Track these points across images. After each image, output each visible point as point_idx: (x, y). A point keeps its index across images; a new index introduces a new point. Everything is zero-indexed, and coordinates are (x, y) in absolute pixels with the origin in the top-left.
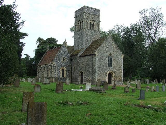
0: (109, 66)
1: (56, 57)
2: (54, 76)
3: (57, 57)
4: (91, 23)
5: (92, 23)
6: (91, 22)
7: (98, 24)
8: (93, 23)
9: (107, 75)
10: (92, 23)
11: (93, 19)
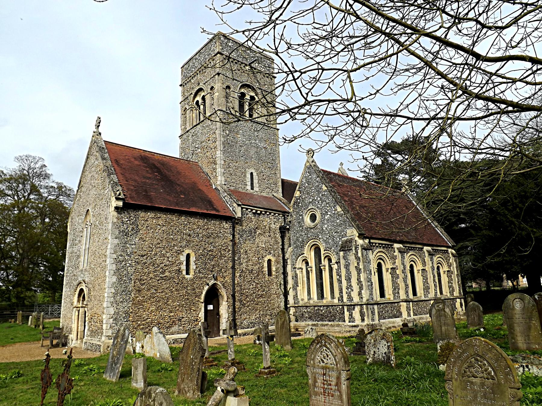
5: (200, 101)
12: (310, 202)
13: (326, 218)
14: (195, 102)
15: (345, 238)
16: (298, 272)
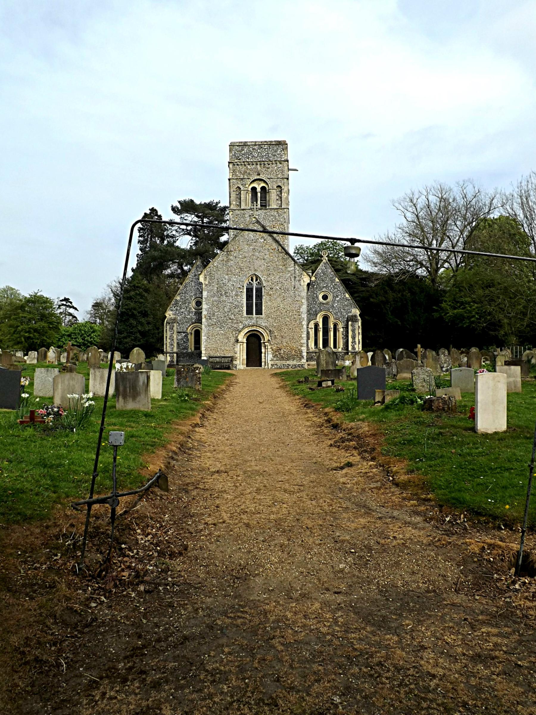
0: (249, 312)
1: (176, 300)
2: (168, 348)
3: (178, 298)
4: (254, 189)
5: (259, 190)
6: (255, 185)
7: (279, 187)
8: (263, 188)
9: (242, 338)
10: (259, 190)
11: (262, 177)
12: (324, 287)
13: (337, 299)
14: (250, 187)
15: (351, 314)
16: (310, 330)
